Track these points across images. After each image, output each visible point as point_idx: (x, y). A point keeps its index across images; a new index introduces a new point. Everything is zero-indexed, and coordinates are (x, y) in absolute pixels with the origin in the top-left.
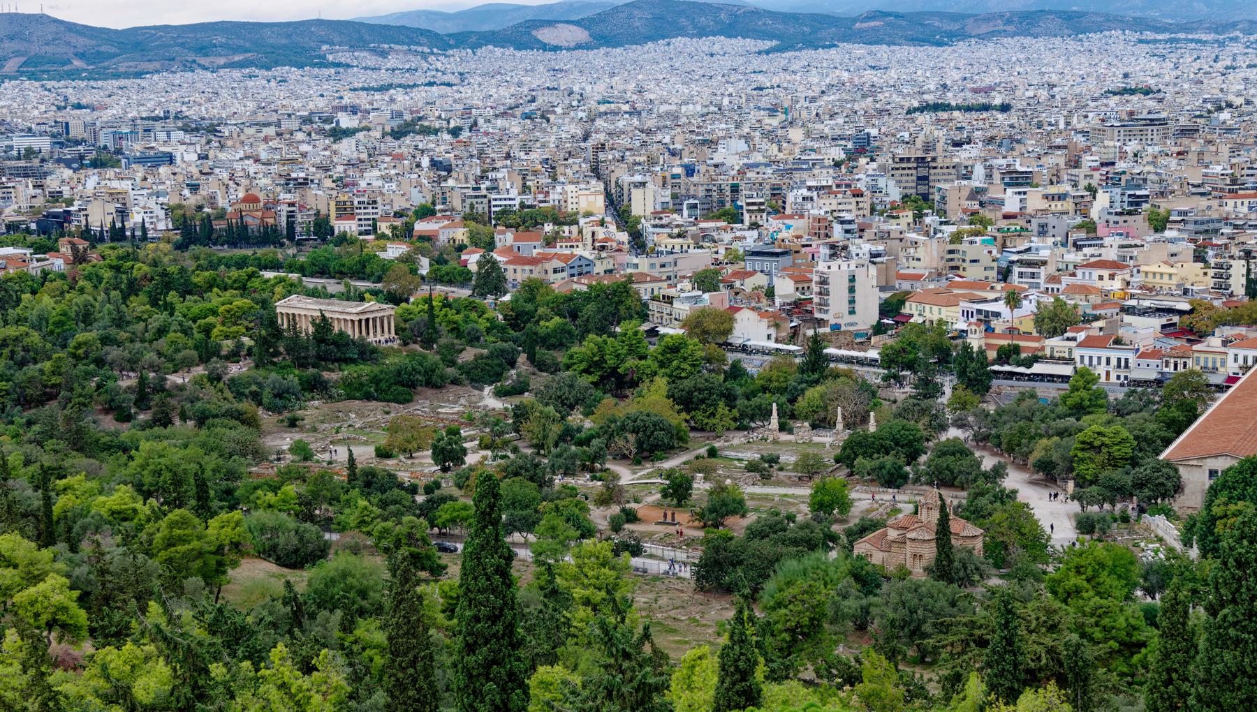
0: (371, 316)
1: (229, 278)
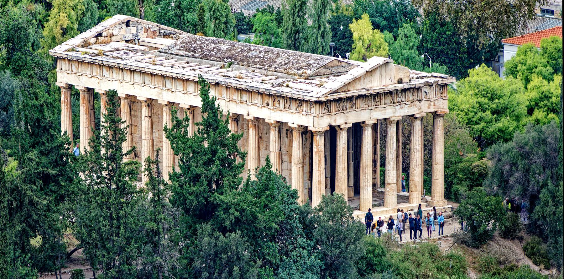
0: (368, 115)
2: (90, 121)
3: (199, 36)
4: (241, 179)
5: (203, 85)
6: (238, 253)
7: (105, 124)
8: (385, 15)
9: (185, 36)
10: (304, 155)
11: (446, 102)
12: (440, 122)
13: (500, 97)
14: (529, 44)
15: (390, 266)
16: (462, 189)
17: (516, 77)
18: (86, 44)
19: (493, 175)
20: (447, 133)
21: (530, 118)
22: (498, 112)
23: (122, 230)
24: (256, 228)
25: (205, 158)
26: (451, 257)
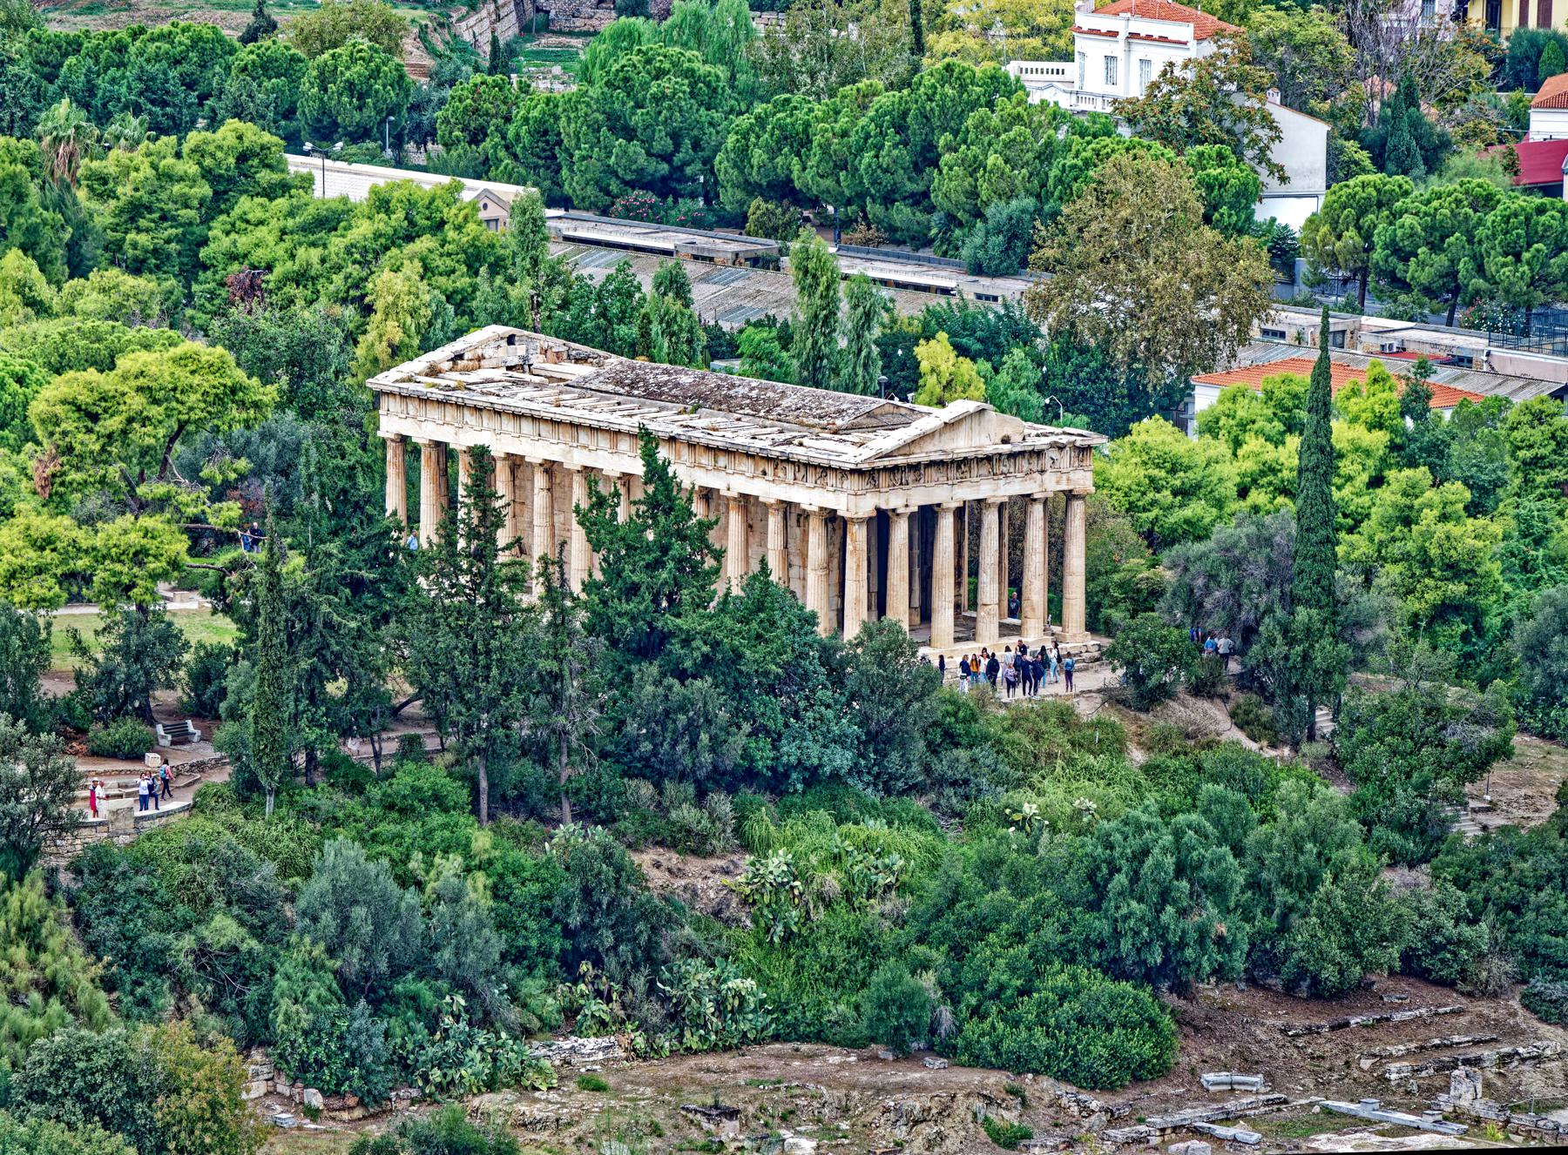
0: (948, 494)
1: (102, 186)
2: (438, 494)
3: (640, 361)
4: (715, 592)
5: (647, 440)
6: (706, 714)
7: (467, 500)
8: (979, 333)
9: (614, 361)
10: (830, 556)
11: (1090, 475)
12: (1078, 508)
13: (1188, 468)
14: (1240, 384)
15: (986, 738)
16: (1117, 615)
17: (1216, 437)
18: (433, 371)
19: (1174, 594)
20: (1091, 524)
21: (1242, 503)
22: (1185, 493)
23: (495, 672)
24: (741, 672)
25: (649, 558)
26: (1098, 725)
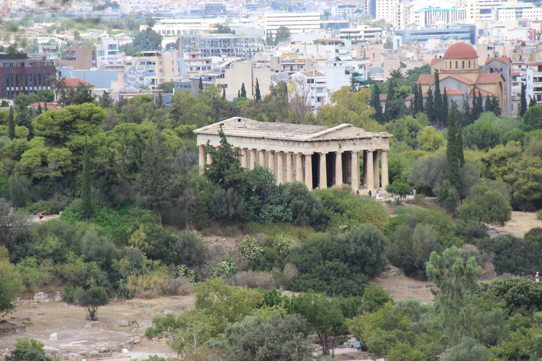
0: (338, 150)
